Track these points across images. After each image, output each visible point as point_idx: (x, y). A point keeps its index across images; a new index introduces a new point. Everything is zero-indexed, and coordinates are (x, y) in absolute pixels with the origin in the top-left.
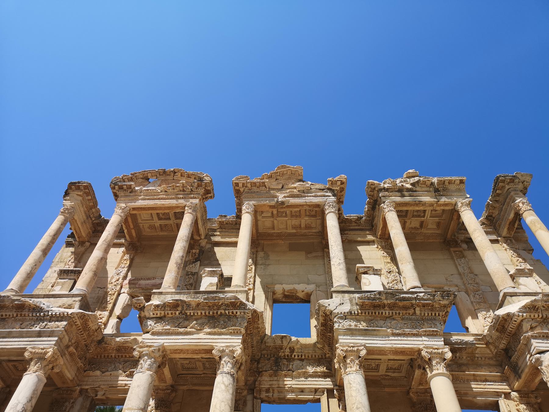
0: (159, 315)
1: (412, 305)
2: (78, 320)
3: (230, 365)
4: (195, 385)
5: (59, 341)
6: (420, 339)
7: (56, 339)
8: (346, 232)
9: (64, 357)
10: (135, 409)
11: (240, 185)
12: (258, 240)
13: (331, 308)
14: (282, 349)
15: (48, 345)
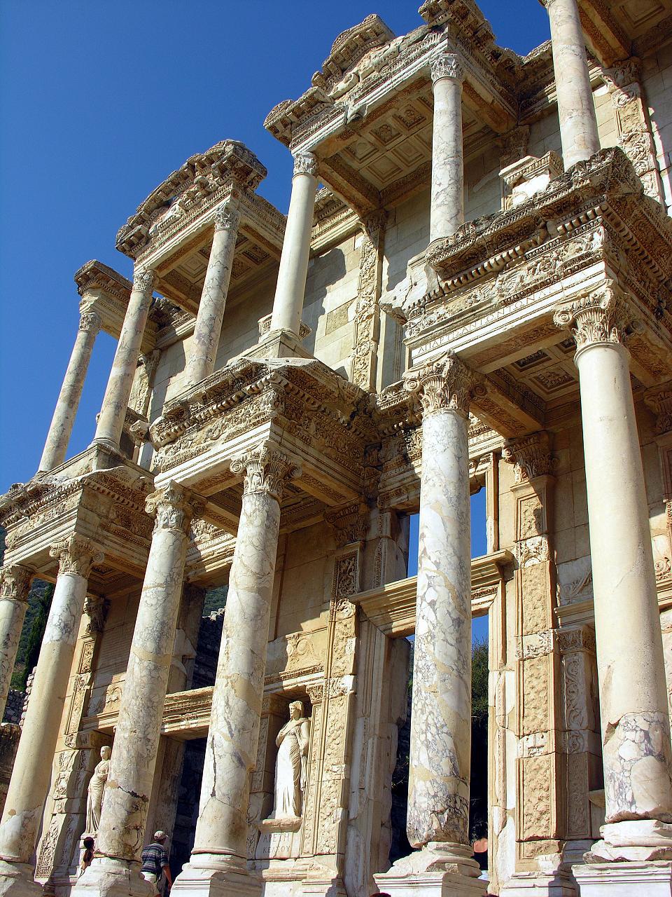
0: (168, 439)
1: (537, 219)
2: (98, 485)
3: (256, 479)
4: (296, 521)
5: (81, 523)
6: (557, 287)
7: (74, 521)
8: (539, 94)
9: (106, 542)
10: (151, 588)
11: (280, 127)
12: (381, 208)
13: (396, 304)
14: (406, 409)
15: (68, 531)
